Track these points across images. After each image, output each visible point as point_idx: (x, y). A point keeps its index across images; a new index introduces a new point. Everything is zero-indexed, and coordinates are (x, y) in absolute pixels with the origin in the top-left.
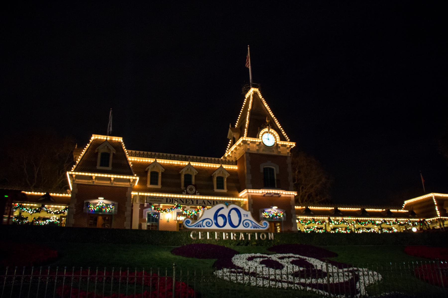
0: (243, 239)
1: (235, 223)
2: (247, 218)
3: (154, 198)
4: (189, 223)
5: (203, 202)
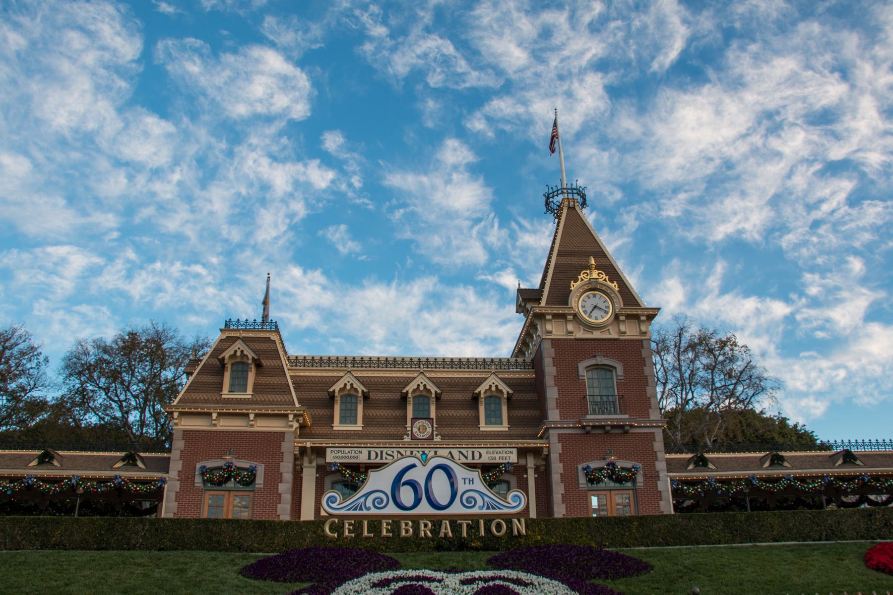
0: (450, 534)
1: (443, 499)
2: (471, 487)
3: (341, 451)
4: (333, 502)
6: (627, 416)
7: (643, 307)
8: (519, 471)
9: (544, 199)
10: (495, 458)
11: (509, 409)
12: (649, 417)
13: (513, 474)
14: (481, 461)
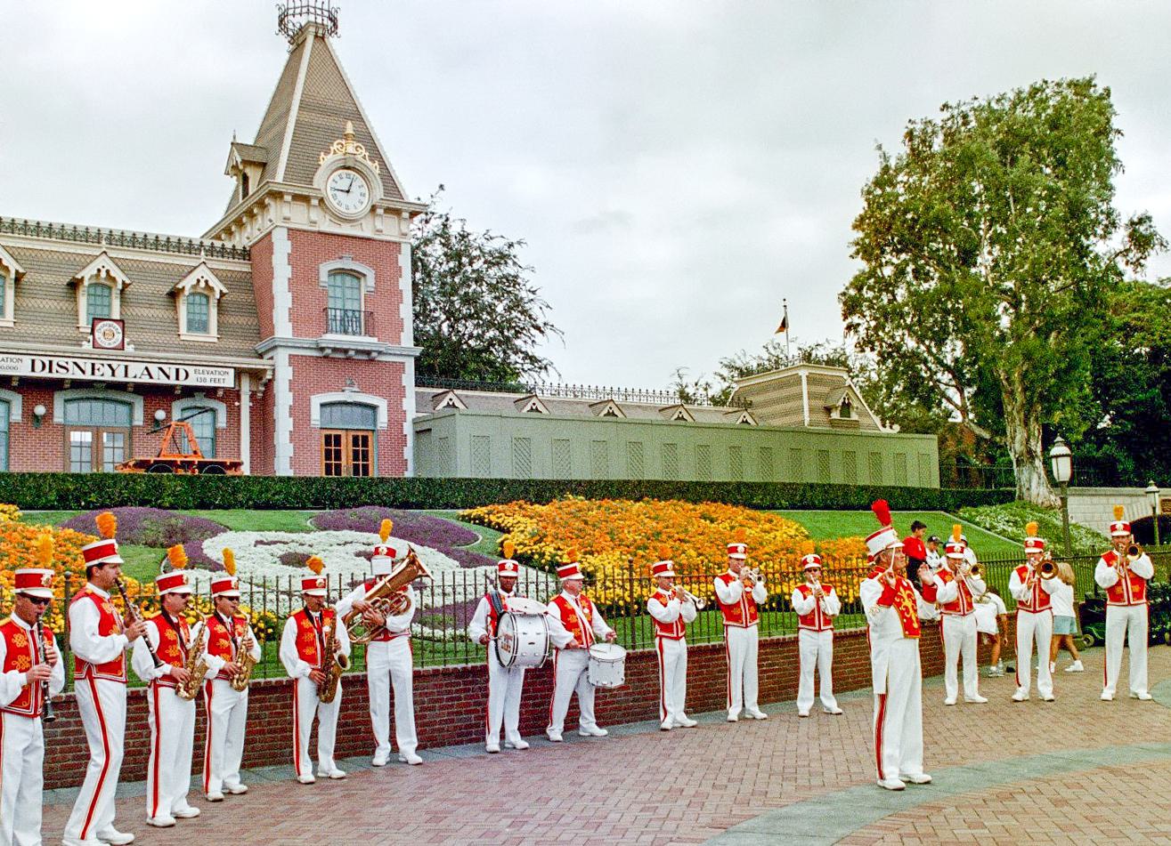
5: (146, 372)
6: (375, 340)
7: (406, 200)
8: (231, 396)
9: (277, 13)
10: (205, 380)
11: (220, 313)
12: (399, 343)
13: (221, 399)
14: (187, 383)
